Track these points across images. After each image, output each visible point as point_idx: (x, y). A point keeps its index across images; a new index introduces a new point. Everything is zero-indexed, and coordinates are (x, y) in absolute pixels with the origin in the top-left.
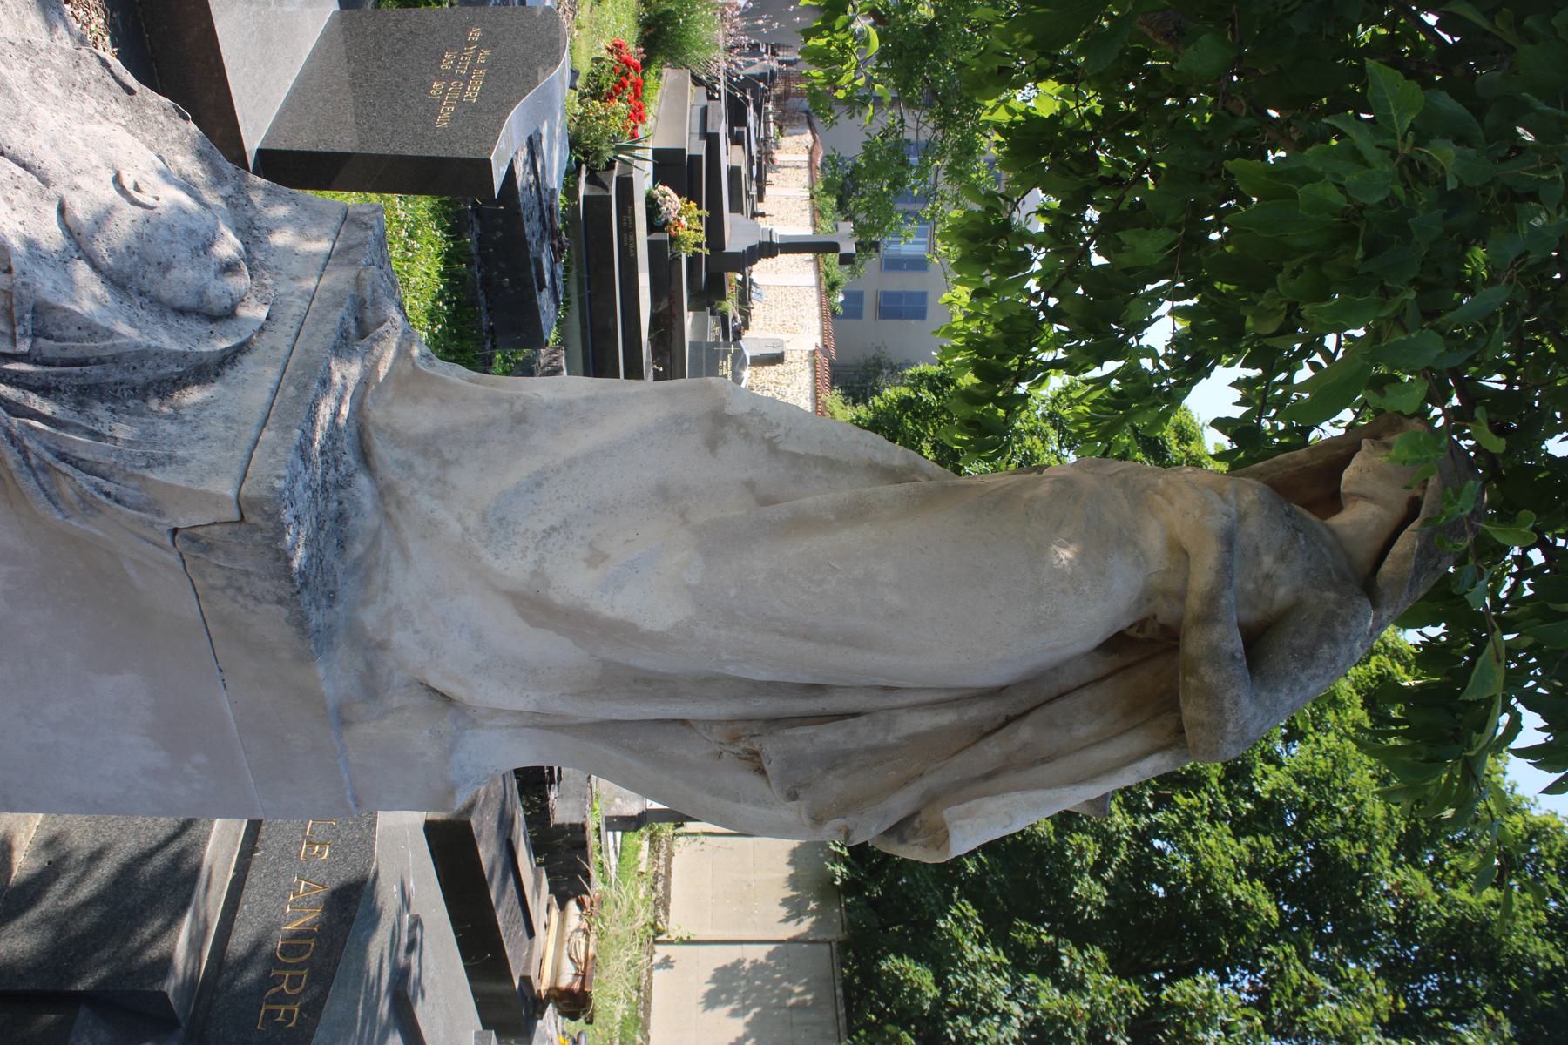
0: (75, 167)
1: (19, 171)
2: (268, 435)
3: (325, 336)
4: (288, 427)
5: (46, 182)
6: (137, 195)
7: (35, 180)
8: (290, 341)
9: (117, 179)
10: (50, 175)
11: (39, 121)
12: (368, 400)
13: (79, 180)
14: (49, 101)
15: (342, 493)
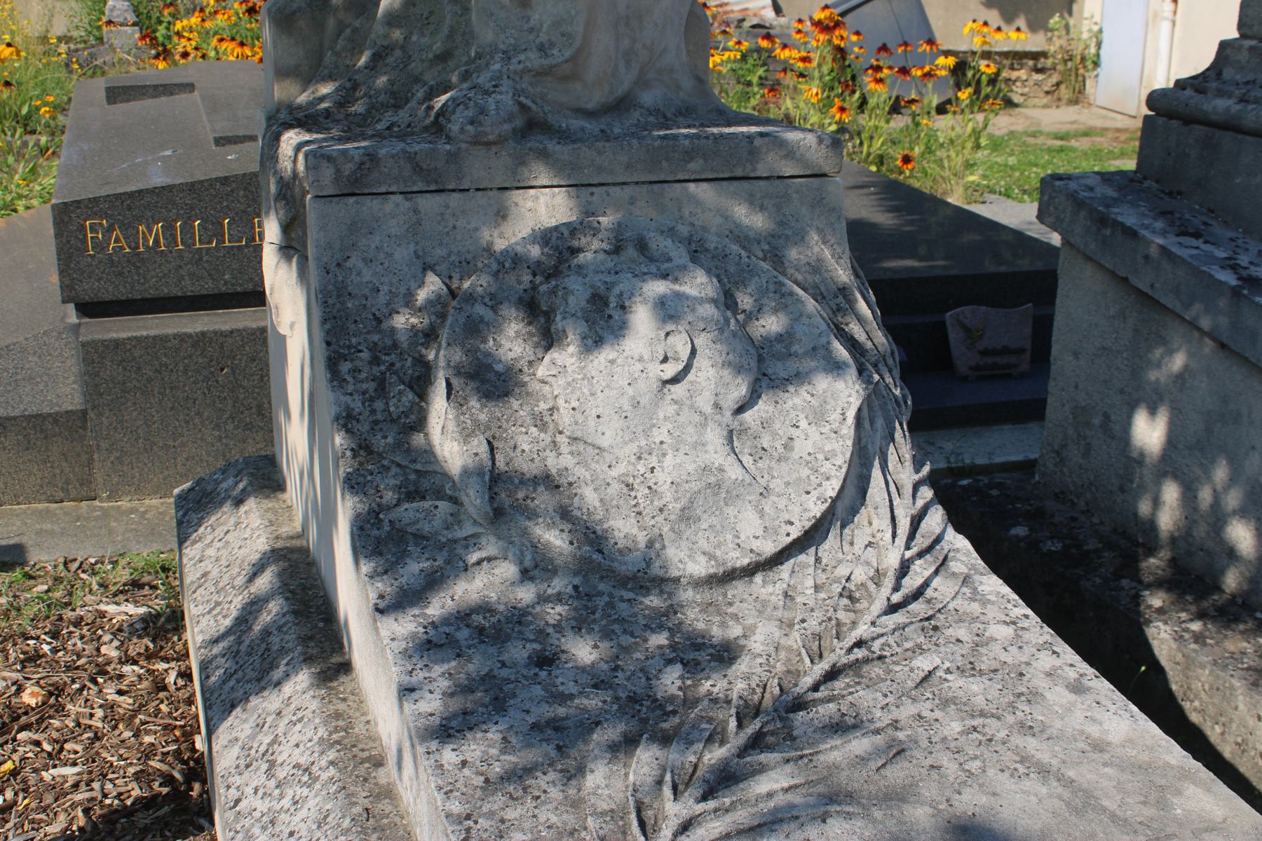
0: (697, 418)
1: (747, 460)
2: (762, 171)
3: (600, 153)
4: (751, 153)
5: (731, 432)
6: (685, 353)
7: (736, 444)
8: (612, 190)
9: (675, 380)
10: (725, 433)
11: (691, 468)
12: (591, 106)
13: (708, 409)
14: (610, 491)
15: (669, 115)
